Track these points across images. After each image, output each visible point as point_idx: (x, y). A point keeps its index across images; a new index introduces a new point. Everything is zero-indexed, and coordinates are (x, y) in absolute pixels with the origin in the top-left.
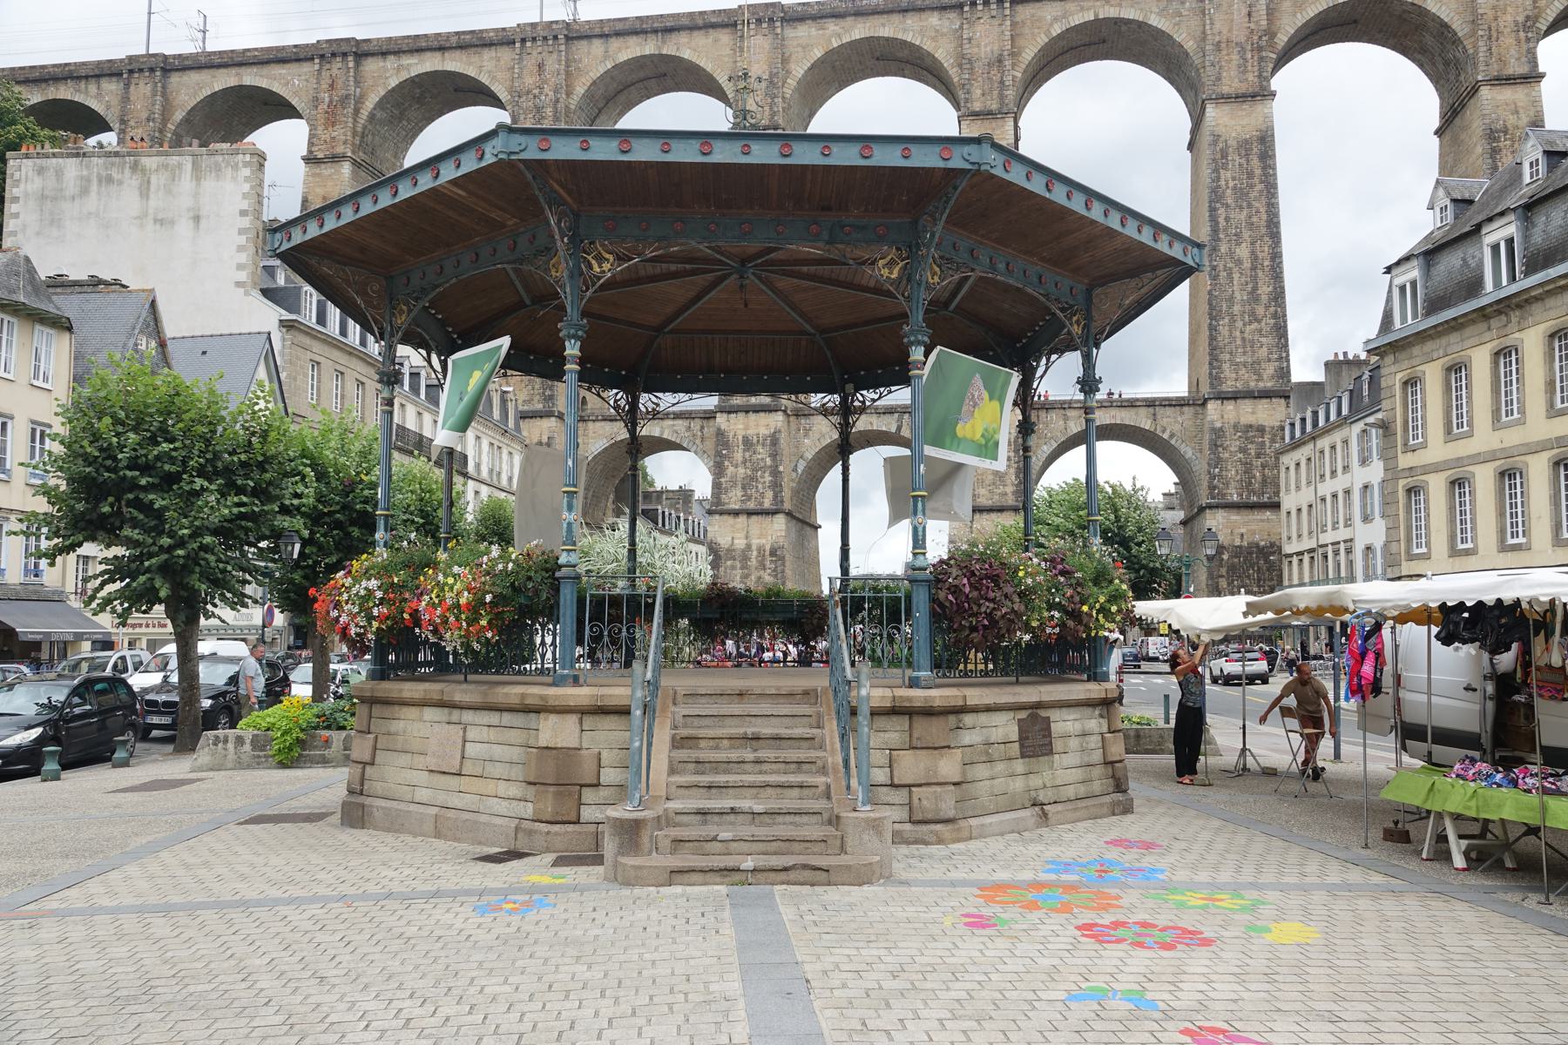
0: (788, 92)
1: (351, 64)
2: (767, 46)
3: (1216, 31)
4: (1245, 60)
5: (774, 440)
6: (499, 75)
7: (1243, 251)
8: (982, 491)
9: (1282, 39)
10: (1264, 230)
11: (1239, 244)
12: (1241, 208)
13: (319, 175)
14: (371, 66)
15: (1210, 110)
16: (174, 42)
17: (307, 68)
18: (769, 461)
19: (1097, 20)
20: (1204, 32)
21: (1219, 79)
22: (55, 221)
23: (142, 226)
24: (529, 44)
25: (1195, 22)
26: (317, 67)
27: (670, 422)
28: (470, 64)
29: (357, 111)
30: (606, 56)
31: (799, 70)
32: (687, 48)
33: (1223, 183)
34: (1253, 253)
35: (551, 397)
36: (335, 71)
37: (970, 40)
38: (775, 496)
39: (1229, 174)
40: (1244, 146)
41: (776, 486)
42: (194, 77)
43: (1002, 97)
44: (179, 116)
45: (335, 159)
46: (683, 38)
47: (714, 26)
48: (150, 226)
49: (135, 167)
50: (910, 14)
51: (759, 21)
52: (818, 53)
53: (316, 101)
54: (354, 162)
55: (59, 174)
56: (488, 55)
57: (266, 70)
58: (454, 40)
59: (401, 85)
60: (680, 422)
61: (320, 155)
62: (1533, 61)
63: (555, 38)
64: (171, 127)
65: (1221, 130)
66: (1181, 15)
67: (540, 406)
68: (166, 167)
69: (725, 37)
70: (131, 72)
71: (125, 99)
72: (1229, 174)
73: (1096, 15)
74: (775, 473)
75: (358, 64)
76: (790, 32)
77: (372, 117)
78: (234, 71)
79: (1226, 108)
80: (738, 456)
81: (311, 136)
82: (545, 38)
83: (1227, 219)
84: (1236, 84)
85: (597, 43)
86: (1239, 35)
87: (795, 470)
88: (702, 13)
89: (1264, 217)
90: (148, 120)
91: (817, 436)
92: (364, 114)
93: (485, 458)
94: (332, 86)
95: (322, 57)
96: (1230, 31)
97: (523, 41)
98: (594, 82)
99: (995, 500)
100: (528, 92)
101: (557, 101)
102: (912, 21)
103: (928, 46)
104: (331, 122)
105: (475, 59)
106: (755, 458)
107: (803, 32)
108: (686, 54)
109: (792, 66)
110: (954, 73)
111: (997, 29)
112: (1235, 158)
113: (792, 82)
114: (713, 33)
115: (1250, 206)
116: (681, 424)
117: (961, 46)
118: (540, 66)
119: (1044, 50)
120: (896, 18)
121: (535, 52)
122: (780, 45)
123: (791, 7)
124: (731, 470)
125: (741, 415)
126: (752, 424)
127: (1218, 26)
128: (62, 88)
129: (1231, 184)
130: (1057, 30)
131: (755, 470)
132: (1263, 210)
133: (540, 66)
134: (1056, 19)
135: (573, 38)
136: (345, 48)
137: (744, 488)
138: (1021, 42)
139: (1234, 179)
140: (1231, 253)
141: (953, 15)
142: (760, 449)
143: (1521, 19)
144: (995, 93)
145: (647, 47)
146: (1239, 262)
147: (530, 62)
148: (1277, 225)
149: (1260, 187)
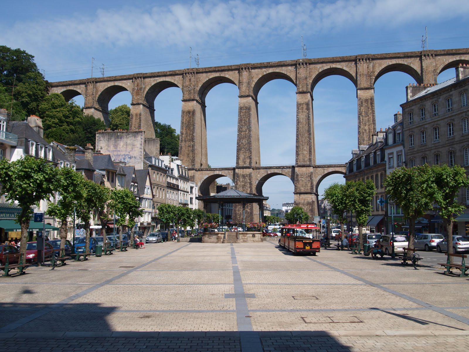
0: (253, 86)
6: (179, 82)
7: (367, 128)
8: (302, 188)
10: (372, 122)
11: (365, 126)
14: (147, 80)
16: (98, 75)
19: (330, 68)
21: (360, 84)
25: (355, 69)
29: (144, 91)
30: (207, 77)
31: (256, 80)
32: (227, 75)
34: (369, 128)
35: (194, 165)
37: (299, 73)
40: (366, 100)
41: (251, 187)
43: (307, 88)
44: (99, 93)
45: (138, 104)
46: (226, 72)
51: (245, 69)
52: (260, 76)
53: (133, 89)
54: (144, 105)
56: (176, 77)
59: (155, 85)
61: (135, 103)
63: (194, 73)
65: (361, 97)
71: (87, 89)
76: (253, 71)
79: (362, 91)
80: (241, 180)
81: (133, 98)
82: (191, 73)
86: (365, 72)
87: (256, 183)
89: (372, 119)
92: (145, 92)
94: (138, 85)
95: (135, 78)
97: (186, 74)
98: (204, 84)
99: (306, 191)
100: (187, 86)
101: (194, 89)
103: (288, 74)
104: (137, 94)
105: (173, 77)
107: (256, 71)
108: (227, 76)
110: (295, 81)
112: (364, 104)
113: (254, 83)
115: (368, 116)
116: (226, 171)
117: (296, 74)
118: (190, 80)
119: (318, 75)
123: (254, 64)
125: (242, 170)
127: (360, 70)
128: (71, 87)
130: (320, 70)
132: (371, 117)
133: (190, 80)
134: (320, 68)
136: (141, 76)
143: (433, 70)
145: (217, 75)
146: (365, 130)
147: (187, 79)
148: (375, 121)
149: (370, 111)
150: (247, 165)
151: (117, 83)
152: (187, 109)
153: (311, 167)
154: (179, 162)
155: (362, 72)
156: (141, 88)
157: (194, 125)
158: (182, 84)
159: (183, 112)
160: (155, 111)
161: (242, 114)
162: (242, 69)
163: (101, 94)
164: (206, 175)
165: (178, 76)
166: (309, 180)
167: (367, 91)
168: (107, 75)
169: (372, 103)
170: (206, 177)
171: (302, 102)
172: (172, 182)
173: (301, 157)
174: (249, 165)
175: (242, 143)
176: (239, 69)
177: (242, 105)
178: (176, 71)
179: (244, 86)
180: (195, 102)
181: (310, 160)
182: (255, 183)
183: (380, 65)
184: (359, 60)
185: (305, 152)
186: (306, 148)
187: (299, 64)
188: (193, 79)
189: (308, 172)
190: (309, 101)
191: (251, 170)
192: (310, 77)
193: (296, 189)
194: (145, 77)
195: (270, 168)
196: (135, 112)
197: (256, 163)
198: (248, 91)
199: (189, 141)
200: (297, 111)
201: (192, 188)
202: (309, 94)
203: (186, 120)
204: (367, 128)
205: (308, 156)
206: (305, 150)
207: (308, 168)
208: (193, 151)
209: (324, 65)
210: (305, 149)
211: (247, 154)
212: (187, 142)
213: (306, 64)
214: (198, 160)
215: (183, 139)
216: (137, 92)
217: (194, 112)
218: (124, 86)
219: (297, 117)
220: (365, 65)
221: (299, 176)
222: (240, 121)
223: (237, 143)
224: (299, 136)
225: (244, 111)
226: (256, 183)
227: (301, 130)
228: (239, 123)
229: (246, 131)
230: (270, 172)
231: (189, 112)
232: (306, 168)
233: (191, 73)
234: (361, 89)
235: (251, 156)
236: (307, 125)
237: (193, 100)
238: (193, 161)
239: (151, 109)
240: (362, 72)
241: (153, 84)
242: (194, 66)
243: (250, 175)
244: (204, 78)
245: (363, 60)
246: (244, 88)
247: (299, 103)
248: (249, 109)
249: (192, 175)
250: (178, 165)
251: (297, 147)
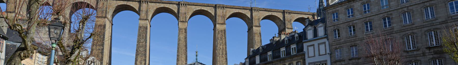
7: (221, 47)
9: (227, 16)
15: (217, 25)
40: (222, 31)
62: (259, 24)
102: (171, 5)
103: (174, 10)
130: (194, 10)
157: (104, 35)
169: (225, 33)
177: (141, 25)
183: (230, 11)
185: (183, 59)
186: (184, 56)
199: (100, 46)
204: (221, 47)
205: (185, 62)
209: (197, 7)
213: (186, 5)
217: (104, 26)
220: (221, 11)
222: (139, 35)
227: (181, 44)
229: (143, 42)
246: (143, 15)
251: (178, 56)
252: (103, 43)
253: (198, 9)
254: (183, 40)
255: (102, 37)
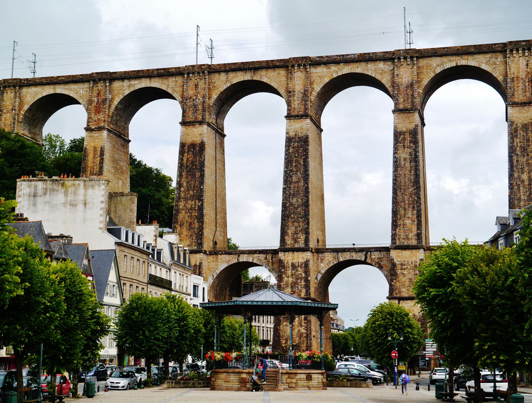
1: (108, 84)
2: (303, 77)
3: (512, 72)
4: (526, 86)
5: (306, 264)
6: (177, 89)
8: (403, 290)
11: (523, 173)
12: (524, 156)
13: (92, 136)
14: (117, 84)
17: (86, 85)
18: (303, 275)
20: (506, 72)
21: (513, 95)
22: (35, 205)
23: (65, 207)
24: (191, 75)
25: (502, 68)
26: (91, 85)
27: (257, 255)
28: (163, 84)
29: (110, 106)
30: (227, 81)
31: (318, 88)
32: (264, 77)
33: (515, 144)
36: (100, 88)
37: (398, 75)
38: (307, 292)
39: (518, 140)
42: (33, 89)
43: (413, 102)
44: (26, 107)
45: (100, 129)
46: (263, 72)
47: (278, 67)
48: (68, 207)
49: (63, 185)
50: (369, 63)
51: (299, 66)
52: (327, 80)
53: (90, 102)
54: (109, 131)
55: (36, 187)
56: (172, 80)
57: (67, 86)
58: (156, 72)
60: (262, 255)
61: (93, 127)
63: (203, 72)
64: (22, 112)
66: (496, 64)
67: (196, 248)
68: (74, 185)
69: (283, 72)
70: (5, 87)
72: (518, 140)
73: (457, 64)
74: (307, 281)
75: (110, 83)
76: (313, 70)
77: (116, 108)
78: (52, 87)
79: (517, 108)
80: (289, 272)
81: (89, 118)
83: (517, 161)
84: (521, 98)
85: (223, 75)
86: (522, 75)
87: (316, 278)
88: (272, 61)
90: (12, 110)
91: (327, 262)
92: (113, 107)
93: (178, 281)
94: (98, 94)
96: (518, 72)
97: (188, 74)
98: (221, 93)
100: (191, 98)
103: (378, 77)
104: (98, 111)
105: (165, 81)
106: (297, 273)
108: (265, 80)
109: (315, 86)
110: (390, 89)
111: (410, 70)
112: (521, 133)
113: (315, 94)
114: (277, 71)
115: (528, 155)
116: (262, 256)
117: (394, 77)
120: (363, 64)
121: (194, 79)
122: (308, 77)
124: (286, 279)
125: (290, 253)
126: (296, 257)
127: (513, 70)
129: (519, 145)
130: (438, 70)
131: (297, 279)
133: (196, 86)
134: (438, 65)
135: (211, 72)
137: (292, 287)
138: (422, 76)
139: (520, 142)
140: (519, 178)
141: (389, 63)
142: (299, 269)
144: (410, 100)
146: (523, 181)
147: (191, 84)
150: (301, 244)
151: (60, 90)
152: (189, 140)
153: (419, 249)
154: (172, 238)
155: (516, 73)
156: (106, 99)
158: (181, 93)
159: (182, 145)
160: (130, 144)
161: (291, 150)
162: (293, 66)
163: (30, 109)
164: (223, 262)
165: (174, 79)
166: (416, 274)
167: (526, 108)
168: (42, 73)
170: (223, 266)
171: (404, 130)
172: (158, 275)
173: (400, 232)
174: (303, 246)
175: (291, 204)
176: (287, 67)
177: (292, 134)
178: (171, 68)
179: (296, 98)
180: (205, 127)
181: (419, 236)
182: (314, 279)
184: (511, 51)
185: (408, 222)
186: (411, 213)
187: (399, 59)
188: (201, 84)
189: (413, 259)
190: (417, 126)
191: (308, 255)
192: (418, 82)
193: (392, 290)
194: (110, 78)
195: (344, 250)
196: (93, 144)
197: (318, 241)
198: (303, 106)
199: (193, 198)
200: (395, 145)
201: (195, 287)
202: (417, 115)
203: (188, 159)
206: (409, 218)
207: (414, 251)
208: (201, 218)
209: (445, 59)
210: (410, 215)
211: (301, 224)
212: (190, 202)
213: (412, 58)
214: (208, 233)
215: (182, 195)
216: (95, 107)
217: (202, 146)
218: (72, 94)
219: (394, 157)
220: (522, 62)
221: (399, 267)
222: (288, 162)
223: (283, 203)
224: (399, 193)
225: (296, 144)
226: (316, 278)
228: (286, 166)
230: (342, 257)
231: (193, 145)
232: (410, 251)
233: (199, 73)
234: (515, 104)
235: (308, 228)
236: (413, 172)
237: (201, 123)
238: (200, 235)
239: (122, 137)
240: (516, 73)
241: (127, 92)
242: (204, 60)
243: (306, 264)
244: (222, 83)
245: (517, 50)
246: (296, 102)
247: (399, 130)
248: (304, 141)
249: (198, 264)
250: (171, 244)
251: (395, 213)
252: (202, 191)
253: (448, 65)
254: (408, 165)
255: (198, 174)
